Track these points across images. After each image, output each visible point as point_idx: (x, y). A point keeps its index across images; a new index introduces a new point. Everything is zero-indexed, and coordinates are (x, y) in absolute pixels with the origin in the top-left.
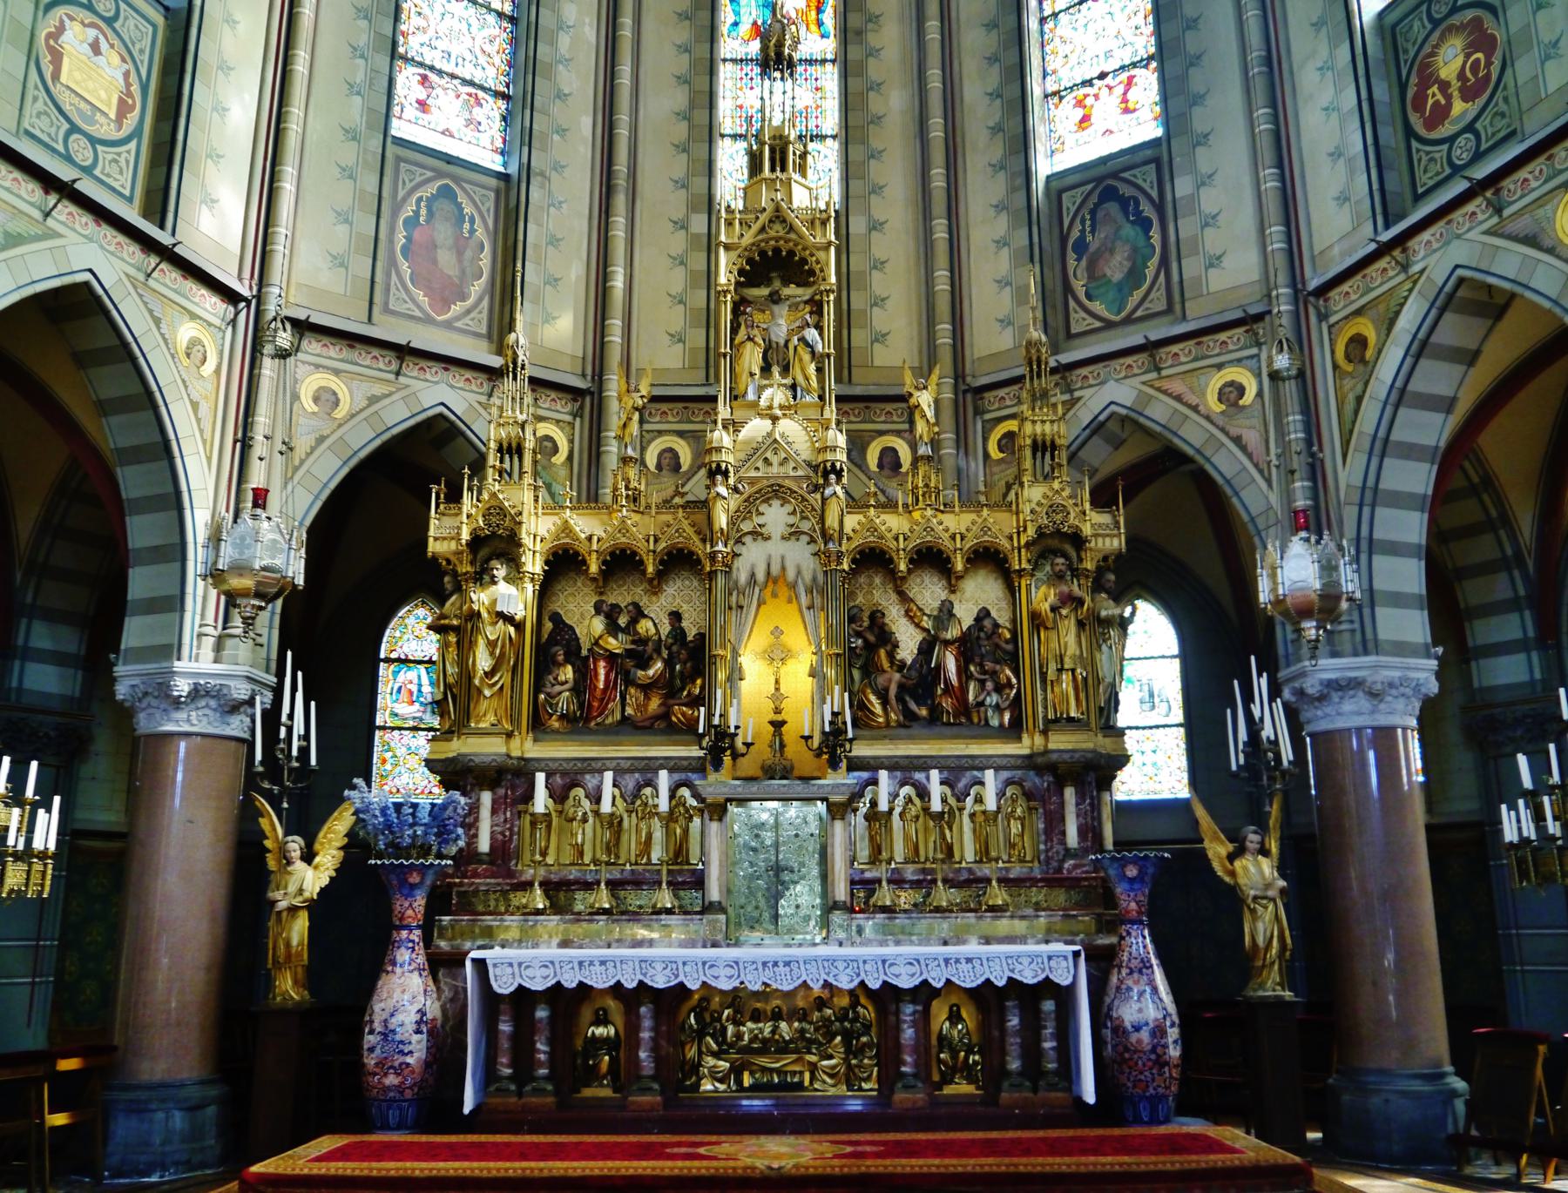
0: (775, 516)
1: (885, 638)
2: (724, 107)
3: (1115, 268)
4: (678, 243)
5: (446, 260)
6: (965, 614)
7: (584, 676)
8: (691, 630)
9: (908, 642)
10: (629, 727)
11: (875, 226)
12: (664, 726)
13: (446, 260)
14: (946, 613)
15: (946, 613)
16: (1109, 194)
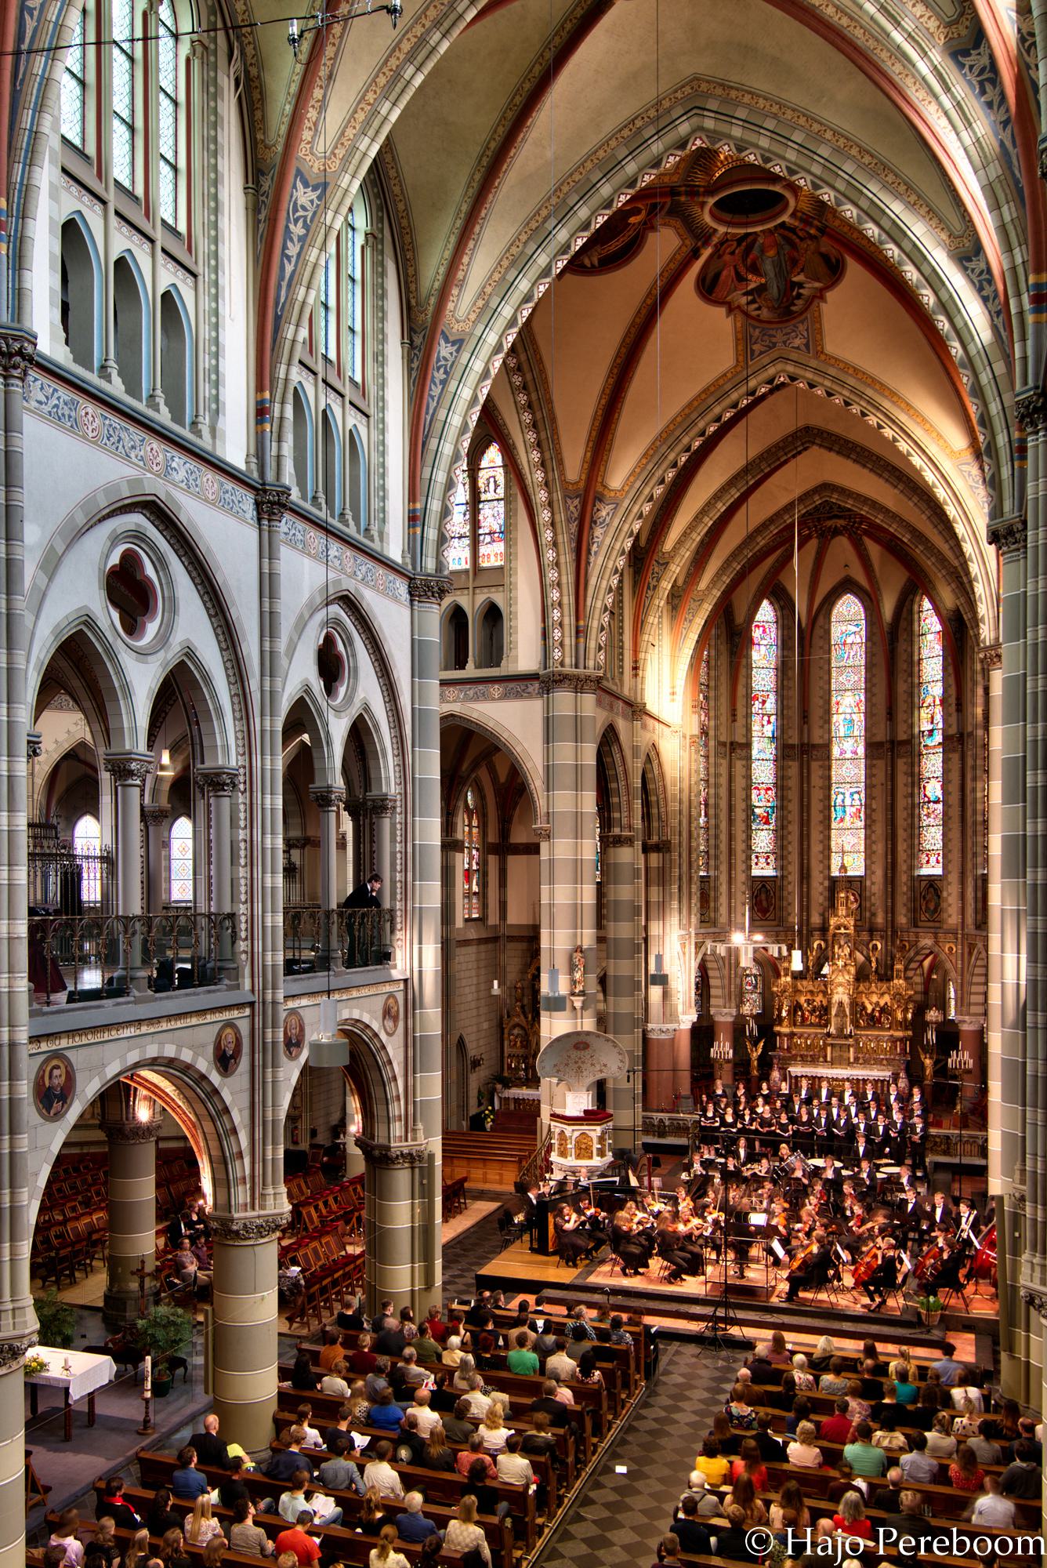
0: (840, 989)
1: (864, 1008)
2: (833, 843)
3: (932, 906)
4: (821, 889)
5: (765, 904)
6: (882, 1003)
7: (803, 1015)
8: (825, 1003)
9: (870, 1008)
10: (812, 1025)
11: (873, 883)
12: (819, 1025)
13: (765, 904)
14: (877, 1004)
15: (877, 1004)
16: (931, 886)
